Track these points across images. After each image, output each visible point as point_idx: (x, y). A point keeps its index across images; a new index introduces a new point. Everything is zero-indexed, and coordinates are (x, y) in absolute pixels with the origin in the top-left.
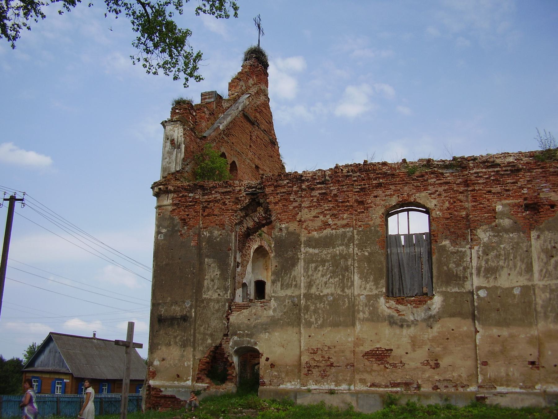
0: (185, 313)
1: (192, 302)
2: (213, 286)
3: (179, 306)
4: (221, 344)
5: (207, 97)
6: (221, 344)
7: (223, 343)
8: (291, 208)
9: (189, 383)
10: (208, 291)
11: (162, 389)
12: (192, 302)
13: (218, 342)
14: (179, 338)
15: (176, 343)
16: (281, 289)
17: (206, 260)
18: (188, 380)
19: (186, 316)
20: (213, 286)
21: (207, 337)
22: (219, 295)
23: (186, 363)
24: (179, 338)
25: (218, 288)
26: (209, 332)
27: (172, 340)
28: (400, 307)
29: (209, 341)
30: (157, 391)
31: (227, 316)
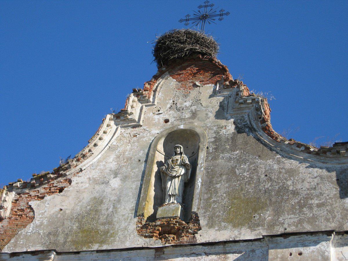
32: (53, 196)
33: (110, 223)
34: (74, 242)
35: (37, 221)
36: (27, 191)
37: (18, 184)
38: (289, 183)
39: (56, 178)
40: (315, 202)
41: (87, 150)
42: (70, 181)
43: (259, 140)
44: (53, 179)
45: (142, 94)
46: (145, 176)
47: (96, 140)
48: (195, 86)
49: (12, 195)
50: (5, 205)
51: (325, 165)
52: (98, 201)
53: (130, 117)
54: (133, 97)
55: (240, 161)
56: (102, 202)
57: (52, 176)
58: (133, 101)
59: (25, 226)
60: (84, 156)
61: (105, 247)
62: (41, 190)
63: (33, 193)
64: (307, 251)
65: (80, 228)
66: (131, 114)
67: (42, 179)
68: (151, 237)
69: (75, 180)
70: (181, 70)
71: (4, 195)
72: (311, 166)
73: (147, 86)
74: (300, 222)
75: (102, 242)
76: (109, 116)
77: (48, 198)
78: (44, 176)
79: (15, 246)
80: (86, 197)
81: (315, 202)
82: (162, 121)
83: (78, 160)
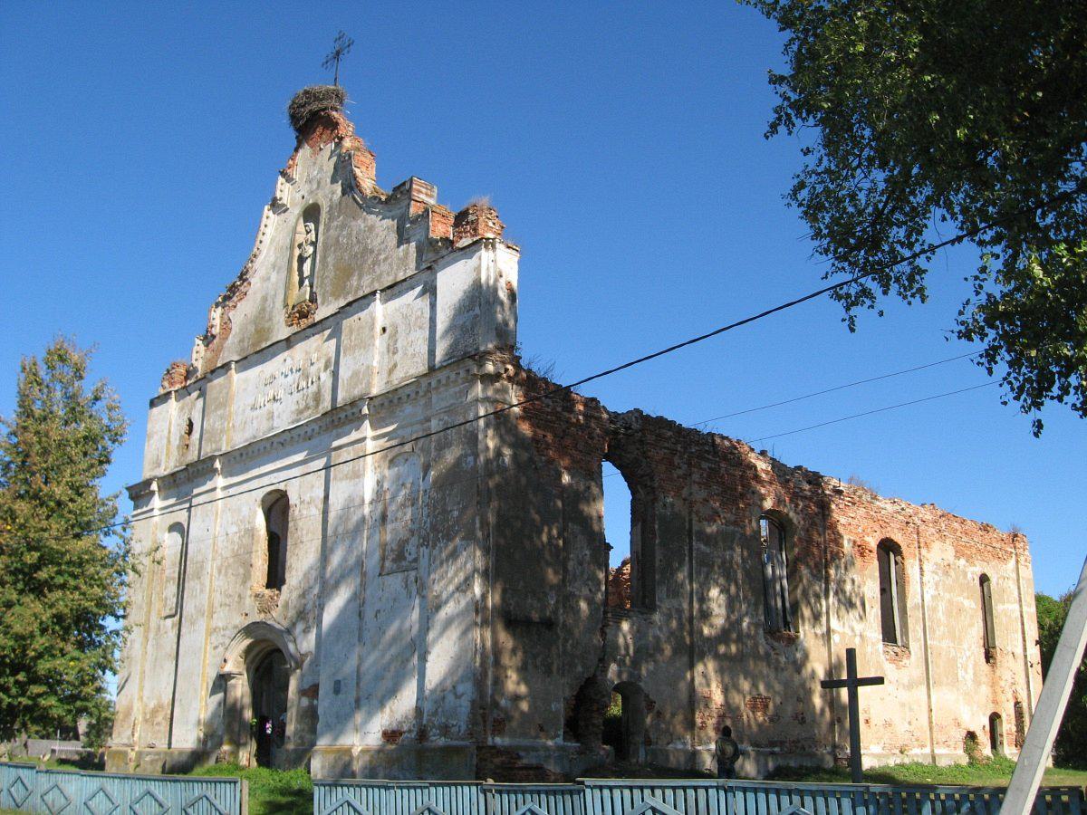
0: (548, 614)
1: (559, 596)
2: (582, 573)
3: (539, 600)
4: (595, 675)
5: (424, 190)
6: (595, 675)
7: (598, 673)
8: (675, 475)
9: (560, 740)
10: (576, 581)
11: (522, 754)
12: (559, 596)
13: (592, 670)
14: (540, 659)
15: (536, 667)
16: (668, 596)
17: (570, 524)
18: (558, 736)
19: (550, 619)
20: (582, 573)
21: (576, 661)
22: (590, 590)
23: (553, 706)
24: (540, 659)
25: (588, 579)
26: (578, 653)
27: (530, 661)
28: (776, 644)
29: (580, 669)
30: (512, 758)
31: (601, 629)
32: (243, 301)
33: (270, 319)
34: (253, 345)
35: (233, 332)
36: (227, 303)
37: (220, 300)
38: (369, 241)
39: (242, 284)
40: (382, 257)
41: (255, 250)
42: (250, 284)
43: (354, 199)
44: (240, 286)
45: (287, 173)
46: (290, 262)
47: (260, 237)
48: (321, 149)
49: (219, 310)
50: (214, 323)
51: (391, 214)
52: (265, 299)
53: (280, 202)
54: (281, 180)
55: (343, 226)
56: (267, 300)
57: (239, 283)
58: (282, 184)
59: (227, 338)
60: (255, 256)
61: (269, 343)
62: (235, 299)
63: (231, 304)
64: (363, 315)
65: (255, 330)
66: (281, 199)
67: (233, 289)
68: (292, 325)
69: (253, 281)
70: (313, 134)
71: (213, 312)
72: (383, 219)
73: (291, 162)
74: (372, 282)
75: (267, 340)
76: (266, 207)
77: (239, 304)
78: (233, 286)
79: (223, 359)
80: (259, 296)
81: (382, 257)
82: (301, 198)
83: (252, 261)
